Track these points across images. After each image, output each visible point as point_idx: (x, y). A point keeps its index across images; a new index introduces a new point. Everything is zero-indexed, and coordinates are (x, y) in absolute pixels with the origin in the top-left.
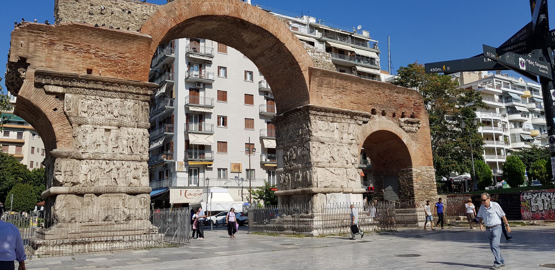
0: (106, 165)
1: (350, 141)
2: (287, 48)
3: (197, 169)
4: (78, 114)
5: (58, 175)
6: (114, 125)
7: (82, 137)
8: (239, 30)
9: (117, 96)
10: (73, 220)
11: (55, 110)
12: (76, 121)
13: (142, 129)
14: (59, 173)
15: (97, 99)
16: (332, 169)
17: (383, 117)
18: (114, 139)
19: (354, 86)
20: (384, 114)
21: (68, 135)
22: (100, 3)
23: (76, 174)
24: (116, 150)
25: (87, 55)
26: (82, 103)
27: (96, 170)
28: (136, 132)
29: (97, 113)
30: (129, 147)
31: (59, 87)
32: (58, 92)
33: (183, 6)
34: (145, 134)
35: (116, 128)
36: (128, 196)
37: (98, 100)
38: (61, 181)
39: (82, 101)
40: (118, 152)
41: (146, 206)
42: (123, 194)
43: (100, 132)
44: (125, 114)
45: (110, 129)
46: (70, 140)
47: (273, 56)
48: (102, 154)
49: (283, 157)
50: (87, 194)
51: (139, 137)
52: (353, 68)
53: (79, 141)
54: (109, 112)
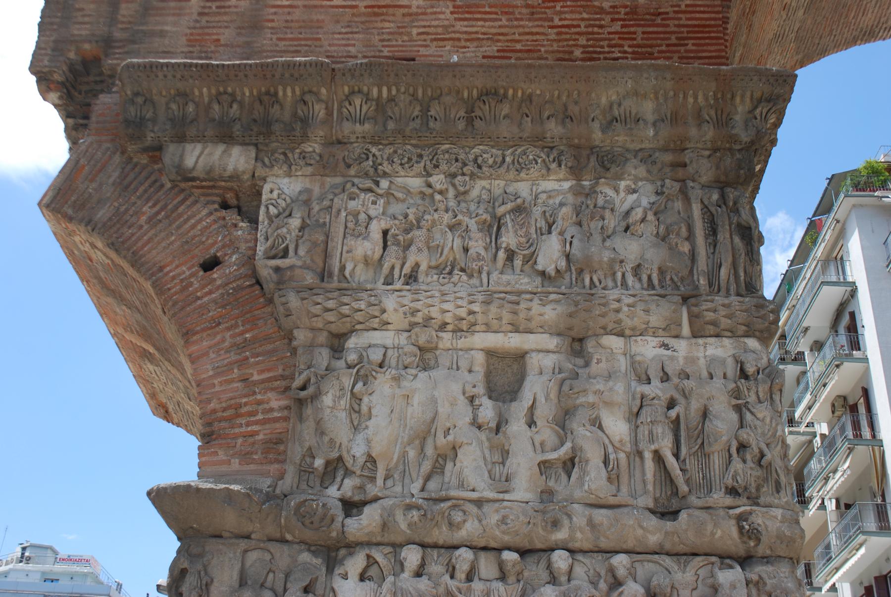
0: (499, 585)
4: (324, 274)
6: (543, 328)
7: (344, 403)
9: (554, 166)
11: (210, 265)
12: (317, 309)
13: (726, 341)
15: (438, 187)
24: (561, 486)
26: (356, 215)
28: (691, 360)
30: (648, 456)
31: (236, 151)
34: (750, 369)
37: (441, 192)
39: (352, 204)
45: (526, 353)
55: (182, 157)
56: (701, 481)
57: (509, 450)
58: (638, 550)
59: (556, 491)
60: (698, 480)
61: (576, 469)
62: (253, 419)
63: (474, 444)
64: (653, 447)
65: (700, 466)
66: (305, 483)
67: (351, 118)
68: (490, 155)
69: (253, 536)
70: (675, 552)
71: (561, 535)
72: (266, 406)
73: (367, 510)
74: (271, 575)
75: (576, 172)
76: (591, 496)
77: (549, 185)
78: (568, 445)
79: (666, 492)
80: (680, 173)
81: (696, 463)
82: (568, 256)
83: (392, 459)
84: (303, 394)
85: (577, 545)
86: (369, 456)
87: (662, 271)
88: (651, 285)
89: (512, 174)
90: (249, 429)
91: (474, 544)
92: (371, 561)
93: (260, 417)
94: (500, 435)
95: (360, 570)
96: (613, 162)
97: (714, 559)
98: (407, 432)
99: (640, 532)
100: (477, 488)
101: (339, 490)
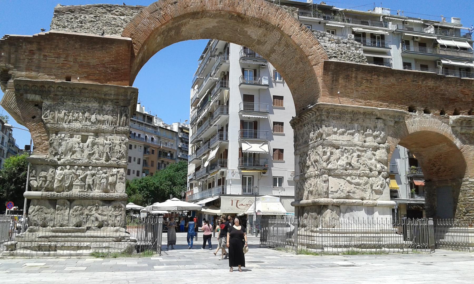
1: (376, 144)
2: (294, 41)
3: (252, 177)
8: (241, 26)
10: (44, 226)
14: (34, 178)
16: (349, 178)
17: (425, 115)
18: (90, 145)
19: (381, 78)
20: (426, 112)
21: (45, 141)
22: (95, 11)
25: (66, 62)
27: (71, 176)
29: (74, 120)
31: (37, 96)
32: (36, 100)
33: (169, 5)
34: (123, 139)
35: (93, 134)
36: (101, 203)
38: (35, 186)
40: (94, 158)
41: (120, 213)
42: (97, 201)
43: (77, 138)
44: (103, 119)
47: (284, 51)
49: (299, 163)
50: (60, 200)
51: (118, 142)
52: (438, 61)
54: (87, 118)
55: (27, 97)
67: (58, 91)
68: (84, 99)
72: (45, 143)
73: (61, 160)
75: (99, 103)
77: (94, 105)
80: (117, 104)
82: (96, 119)
84: (51, 142)
87: (112, 122)
88: (110, 125)
89: (88, 103)
96: (106, 101)
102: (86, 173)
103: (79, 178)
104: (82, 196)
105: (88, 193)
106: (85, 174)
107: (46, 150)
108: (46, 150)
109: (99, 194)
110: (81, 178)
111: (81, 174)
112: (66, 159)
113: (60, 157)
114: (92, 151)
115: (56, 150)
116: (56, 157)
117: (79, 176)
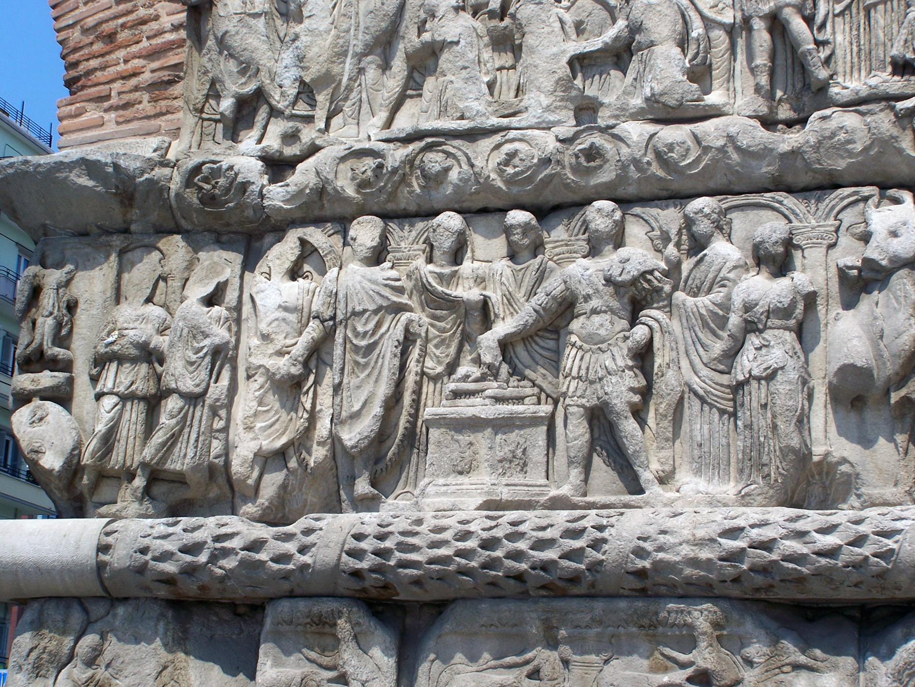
5: (36, 402)
14: (47, 379)
23: (188, 384)
30: (758, 25)
38: (52, 461)
40: (637, 102)
46: (172, 59)
48: (453, 145)
50: (285, 606)
53: (235, 42)
56: (856, 60)
57: (520, 46)
58: (737, 188)
59: (601, 104)
60: (849, 57)
61: (634, 66)
62: (134, 49)
63: (462, 42)
64: (766, 8)
65: (855, 32)
66: (211, 138)
69: (133, 227)
70: (802, 185)
71: (606, 175)
72: (154, 26)
73: (300, 167)
74: (162, 284)
76: (655, 105)
78: (621, 23)
79: (794, 86)
81: (847, 29)
83: (340, 81)
85: (631, 190)
86: (302, 82)
90: (130, 65)
91: (465, 205)
92: (307, 250)
93: (145, 43)
94: (507, 21)
95: (288, 265)
97: (866, 190)
98: (360, 37)
99: (735, 156)
100: (467, 114)
101: (259, 141)
102: (553, 285)
103: (489, 340)
104: (517, 556)
105: (592, 518)
106: (540, 298)
107: (158, 87)
108: (158, 87)
109: (720, 519)
110: (505, 345)
111: (510, 300)
112: (339, 150)
113: (291, 137)
114: (610, 33)
115: (247, 68)
116: (249, 142)
117: (487, 322)
